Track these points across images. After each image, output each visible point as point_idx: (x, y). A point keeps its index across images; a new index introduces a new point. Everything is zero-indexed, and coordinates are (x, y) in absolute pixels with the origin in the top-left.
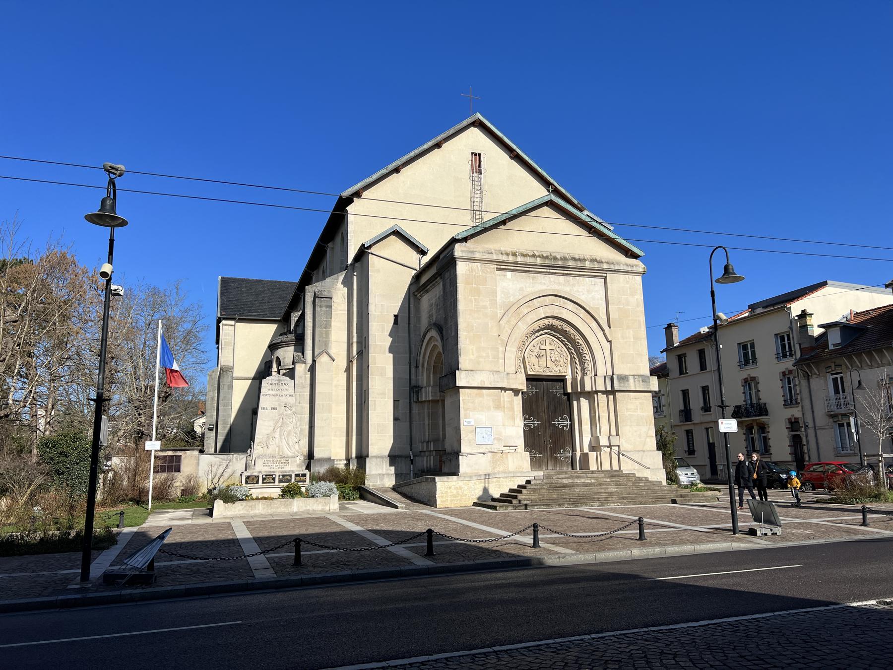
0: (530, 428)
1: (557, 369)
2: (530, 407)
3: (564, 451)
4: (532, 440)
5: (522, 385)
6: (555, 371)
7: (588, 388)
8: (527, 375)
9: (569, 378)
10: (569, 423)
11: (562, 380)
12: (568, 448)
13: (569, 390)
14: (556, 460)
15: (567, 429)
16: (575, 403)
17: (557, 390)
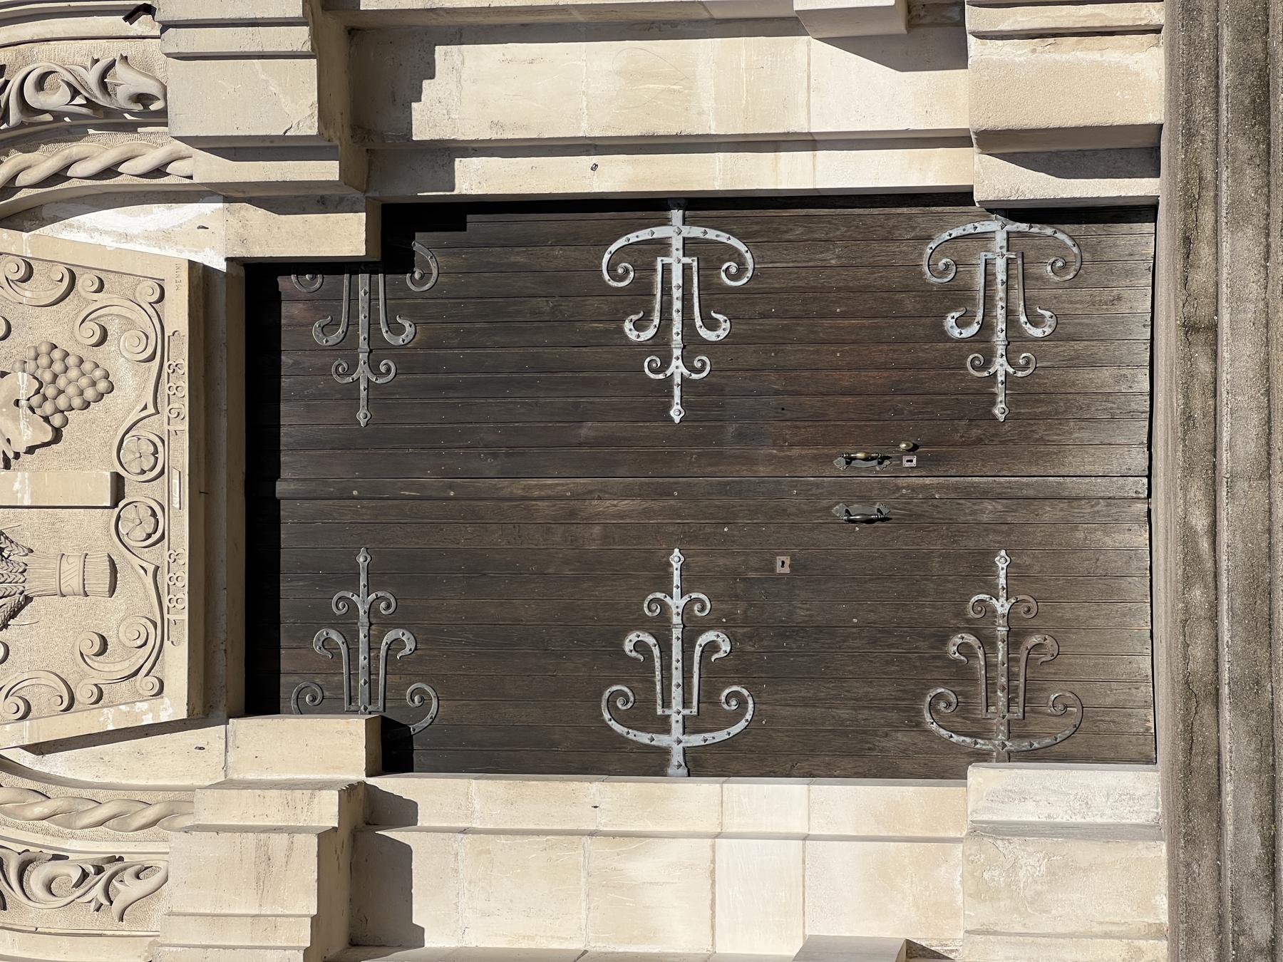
0: (738, 668)
1: (132, 386)
2: (536, 699)
3: (957, 295)
4: (862, 679)
5: (320, 751)
6: (146, 406)
7: (288, 98)
8: (204, 711)
9: (216, 237)
10: (675, 229)
11: (247, 312)
12: (933, 263)
13: (346, 235)
14: (1046, 408)
15: (743, 261)
16: (474, 178)
17: (346, 361)
